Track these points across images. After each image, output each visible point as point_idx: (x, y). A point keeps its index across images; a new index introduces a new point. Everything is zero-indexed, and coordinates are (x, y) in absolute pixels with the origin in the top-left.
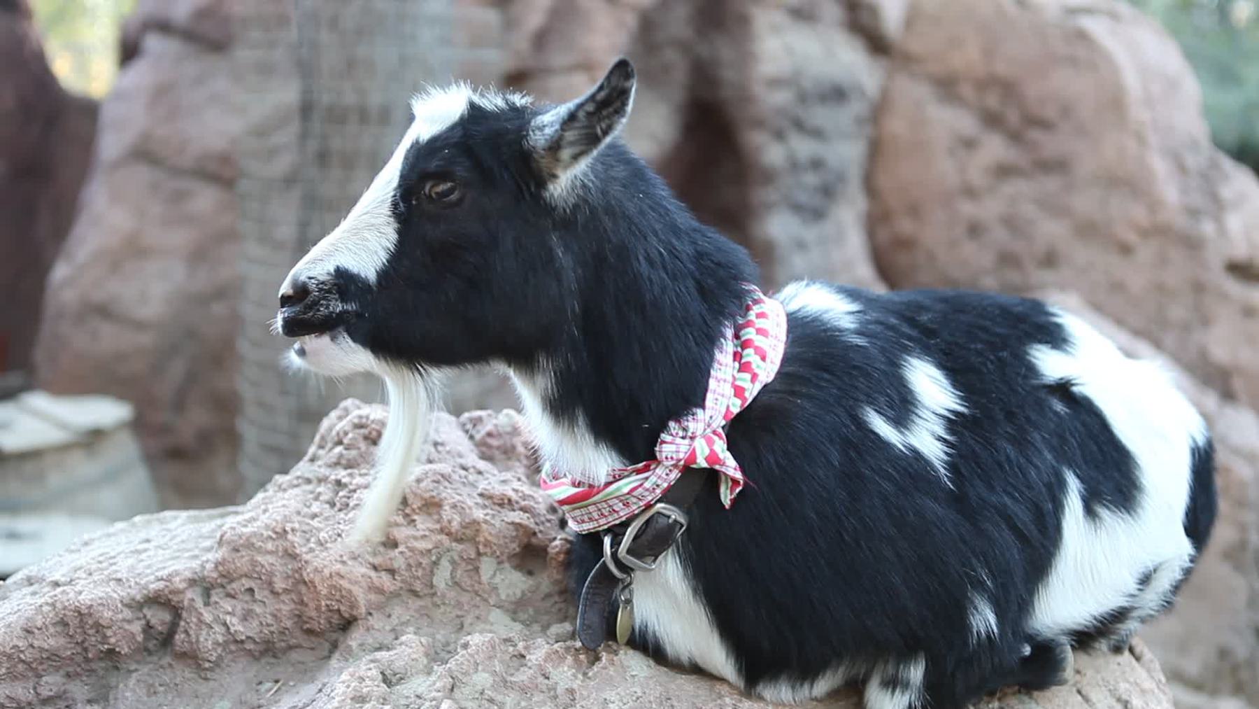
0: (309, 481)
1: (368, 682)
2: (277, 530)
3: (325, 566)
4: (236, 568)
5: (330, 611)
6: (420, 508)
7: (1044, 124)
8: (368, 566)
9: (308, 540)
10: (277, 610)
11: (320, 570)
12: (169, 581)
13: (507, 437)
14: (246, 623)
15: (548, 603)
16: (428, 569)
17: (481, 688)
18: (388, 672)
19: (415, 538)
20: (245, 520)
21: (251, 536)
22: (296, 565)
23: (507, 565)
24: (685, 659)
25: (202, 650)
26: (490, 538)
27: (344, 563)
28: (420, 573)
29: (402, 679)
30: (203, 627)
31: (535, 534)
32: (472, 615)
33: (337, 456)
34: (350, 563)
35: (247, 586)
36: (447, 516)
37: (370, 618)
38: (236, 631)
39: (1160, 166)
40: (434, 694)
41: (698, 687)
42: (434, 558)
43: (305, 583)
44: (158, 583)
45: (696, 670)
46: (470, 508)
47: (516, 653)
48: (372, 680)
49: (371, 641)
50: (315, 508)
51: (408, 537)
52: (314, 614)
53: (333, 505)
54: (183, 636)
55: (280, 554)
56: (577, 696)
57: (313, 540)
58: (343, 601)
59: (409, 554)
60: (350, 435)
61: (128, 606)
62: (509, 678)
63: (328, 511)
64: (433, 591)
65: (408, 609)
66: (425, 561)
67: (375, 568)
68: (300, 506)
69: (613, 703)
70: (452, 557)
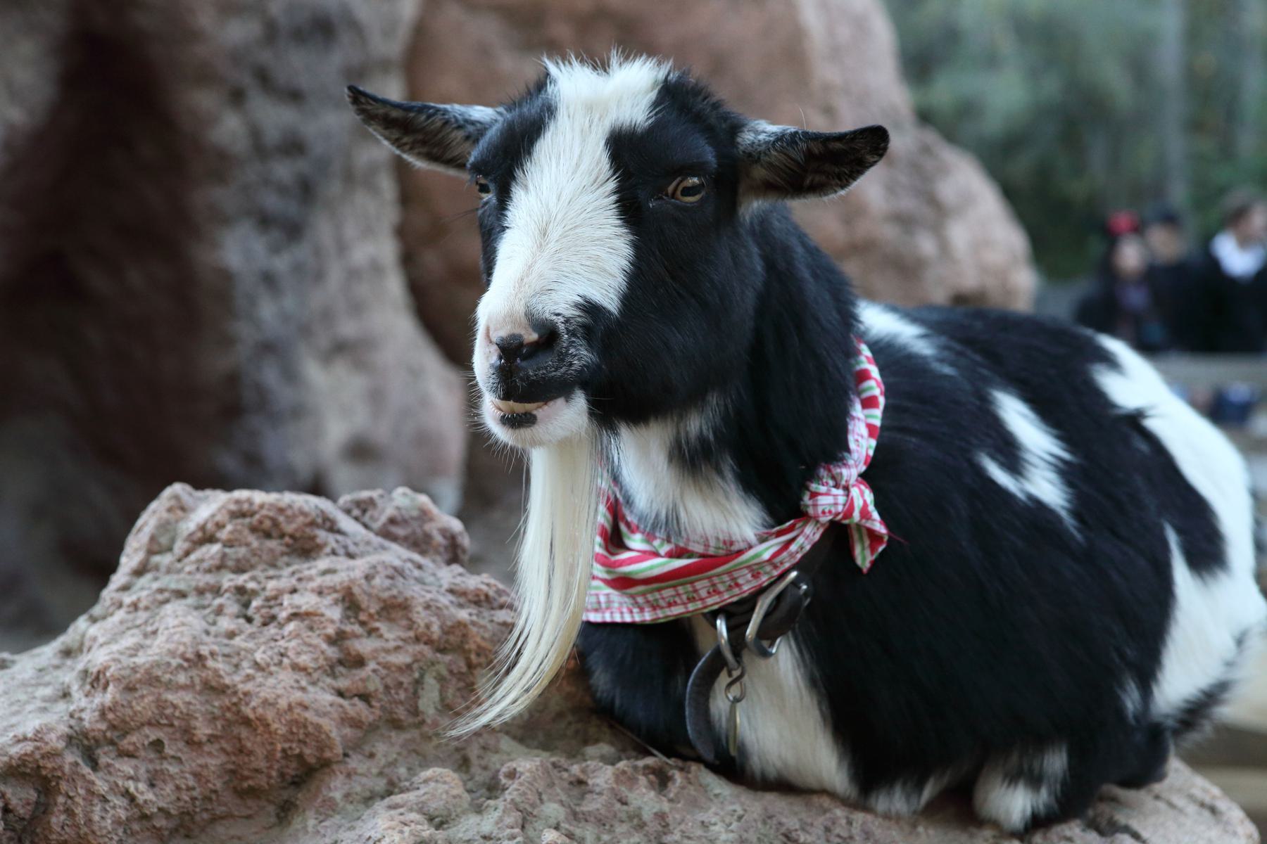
2: (189, 655)
3: (279, 696)
4: (135, 713)
6: (378, 613)
8: (333, 691)
9: (237, 666)
10: (201, 766)
11: (271, 701)
12: (41, 739)
13: (415, 524)
14: (156, 790)
15: (562, 725)
16: (411, 690)
17: (555, 822)
19: (387, 651)
20: (128, 648)
21: (152, 667)
24: (772, 773)
25: (98, 833)
26: (484, 644)
27: (303, 689)
28: (402, 695)
30: (96, 801)
33: (219, 556)
34: (311, 689)
35: (153, 737)
36: (422, 619)
38: (145, 802)
40: (508, 831)
41: (791, 804)
42: (417, 675)
44: (21, 745)
45: (784, 786)
46: (447, 607)
47: (572, 779)
49: (358, 789)
50: (225, 623)
51: (376, 651)
52: (262, 764)
53: (249, 620)
54: (63, 817)
55: (198, 688)
56: (670, 820)
57: (245, 664)
58: (308, 740)
59: (384, 672)
60: (229, 527)
62: (578, 809)
64: (420, 718)
65: (392, 744)
66: (406, 680)
67: (340, 694)
68: (204, 625)
69: (715, 824)
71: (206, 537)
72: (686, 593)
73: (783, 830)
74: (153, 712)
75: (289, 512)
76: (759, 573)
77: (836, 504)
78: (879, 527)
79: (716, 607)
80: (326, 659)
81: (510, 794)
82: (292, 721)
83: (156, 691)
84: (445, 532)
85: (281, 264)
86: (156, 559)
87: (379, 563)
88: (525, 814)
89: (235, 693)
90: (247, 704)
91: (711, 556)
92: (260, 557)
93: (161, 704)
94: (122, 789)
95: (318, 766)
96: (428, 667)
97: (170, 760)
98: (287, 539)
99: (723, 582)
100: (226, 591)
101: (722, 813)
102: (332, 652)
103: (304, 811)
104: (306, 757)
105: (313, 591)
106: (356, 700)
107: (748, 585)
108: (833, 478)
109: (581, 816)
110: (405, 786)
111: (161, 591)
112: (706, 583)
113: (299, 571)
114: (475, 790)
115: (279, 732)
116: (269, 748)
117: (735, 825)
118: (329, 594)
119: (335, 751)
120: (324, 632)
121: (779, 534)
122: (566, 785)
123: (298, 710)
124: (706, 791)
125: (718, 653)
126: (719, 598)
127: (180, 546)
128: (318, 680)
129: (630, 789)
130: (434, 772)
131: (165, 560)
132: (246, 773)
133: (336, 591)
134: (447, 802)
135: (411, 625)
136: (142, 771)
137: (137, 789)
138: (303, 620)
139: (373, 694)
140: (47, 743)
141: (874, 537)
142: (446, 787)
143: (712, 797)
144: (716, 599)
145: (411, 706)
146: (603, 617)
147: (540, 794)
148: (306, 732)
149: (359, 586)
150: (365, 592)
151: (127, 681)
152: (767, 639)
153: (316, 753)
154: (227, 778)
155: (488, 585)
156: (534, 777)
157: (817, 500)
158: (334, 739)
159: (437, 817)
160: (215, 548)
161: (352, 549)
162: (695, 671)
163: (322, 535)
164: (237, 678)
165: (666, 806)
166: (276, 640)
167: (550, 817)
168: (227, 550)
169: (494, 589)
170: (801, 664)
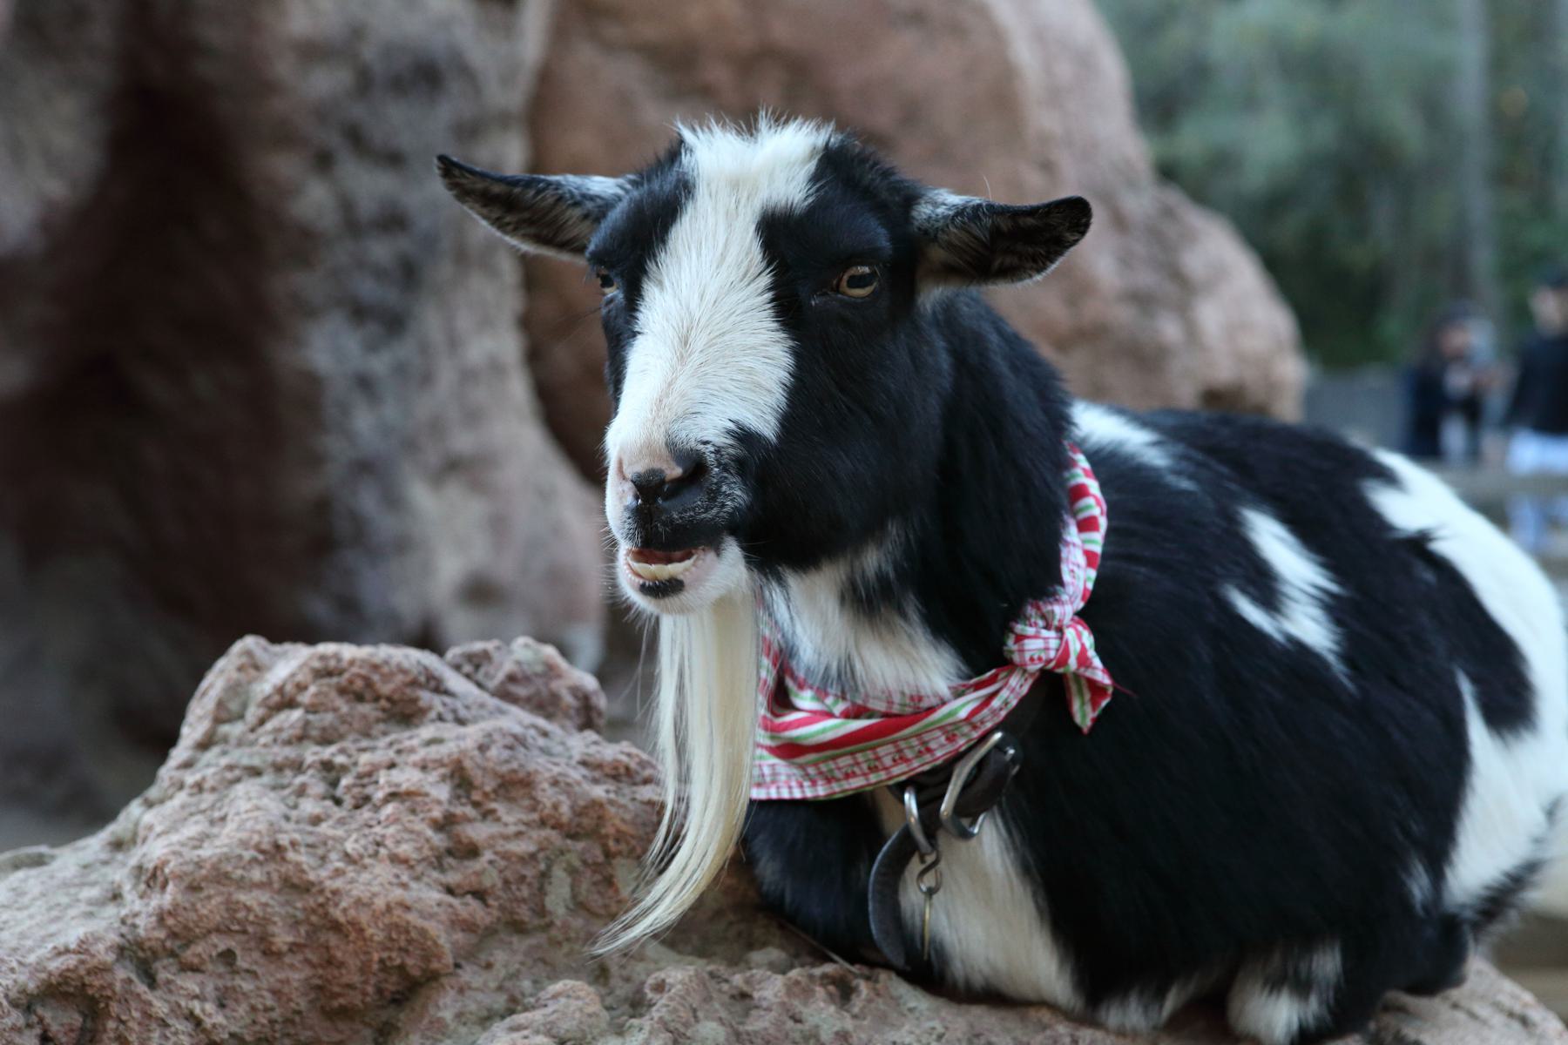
2: (266, 846)
3: (375, 895)
4: (201, 917)
6: (495, 791)
8: (440, 888)
9: (323, 859)
10: (282, 982)
11: (365, 900)
12: (87, 951)
13: (539, 682)
14: (228, 1012)
16: (536, 885)
19: (506, 838)
20: (191, 839)
21: (220, 861)
22: (311, 902)
24: (978, 981)
26: (624, 827)
27: (404, 886)
28: (525, 892)
30: (154, 1026)
33: (300, 724)
34: (413, 885)
35: (222, 947)
37: (459, 971)
38: (214, 1026)
41: (1003, 1019)
42: (542, 866)
44: (62, 959)
46: (579, 784)
47: (735, 992)
49: (473, 1007)
50: (309, 807)
51: (492, 837)
52: (356, 979)
53: (338, 802)
55: (276, 886)
57: (333, 856)
58: (411, 948)
59: (503, 863)
60: (313, 689)
61: (15, 1004)
62: (741, 1028)
64: (547, 920)
65: (514, 952)
67: (450, 890)
68: (283, 809)
70: (569, 863)
71: (284, 701)
72: (866, 761)
74: (222, 917)
75: (386, 669)
76: (954, 735)
77: (1047, 649)
78: (1102, 677)
79: (903, 778)
80: (432, 849)
81: (658, 1011)
82: (391, 924)
83: (224, 889)
84: (576, 691)
85: (379, 364)
86: (225, 729)
87: (495, 730)
88: (676, 1036)
89: (322, 892)
90: (336, 905)
91: (896, 716)
92: (351, 724)
93: (233, 906)
94: (186, 1011)
95: (423, 980)
96: (557, 856)
97: (243, 974)
98: (383, 703)
99: (911, 747)
100: (309, 767)
101: (918, 1031)
103: (407, 1035)
104: (408, 969)
105: (415, 765)
106: (469, 898)
107: (941, 752)
108: (1043, 617)
109: (745, 1037)
110: (529, 1003)
111: (230, 768)
112: (890, 748)
113: (398, 741)
114: (615, 1006)
115: (376, 938)
116: (363, 957)
118: (434, 769)
119: (443, 961)
120: (429, 815)
121: (978, 687)
122: (726, 998)
123: (398, 912)
124: (898, 1005)
125: (907, 834)
126: (908, 766)
127: (253, 713)
128: (423, 874)
129: (805, 1004)
130: (565, 985)
131: (235, 730)
132: (336, 989)
133: (443, 765)
134: (581, 1022)
135: (535, 806)
136: (210, 988)
137: (203, 1011)
138: (403, 802)
139: (490, 891)
140: (93, 956)
141: (1096, 689)
142: (580, 1003)
143: (906, 1012)
144: (903, 768)
145: (537, 905)
146: (768, 793)
147: (694, 1011)
148: (409, 938)
149: (472, 758)
150: (479, 767)
151: (191, 878)
152: (967, 816)
153: (419, 963)
154: (312, 995)
155: (629, 755)
156: (687, 989)
157: (1023, 645)
158: (443, 947)
159: (569, 1040)
160: (296, 715)
161: (463, 713)
162: (880, 857)
163: (425, 697)
164: (324, 873)
165: (849, 1024)
166: (371, 827)
167: (707, 1039)
168: (311, 717)
169: (637, 760)
170: (1010, 847)
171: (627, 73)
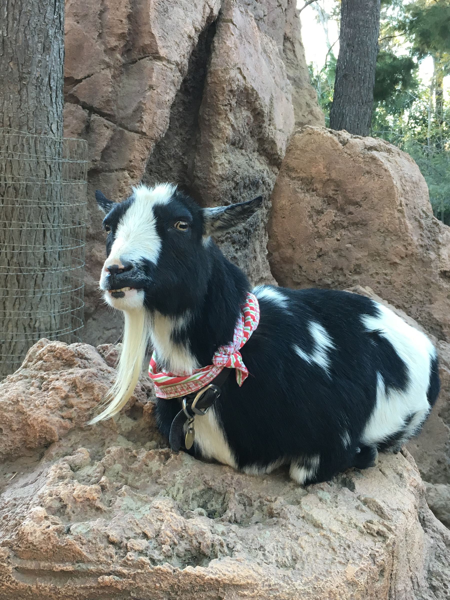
0: (26, 377)
1: (64, 470)
5: (41, 438)
6: (83, 389)
7: (357, 204)
9: (30, 405)
15: (144, 433)
18: (73, 465)
19: (82, 403)
22: (24, 417)
23: (125, 415)
27: (48, 415)
29: (79, 468)
31: (137, 401)
32: (109, 438)
34: (51, 415)
39: (410, 225)
43: (29, 425)
45: (214, 461)
48: (66, 468)
49: (62, 452)
50: (32, 389)
51: (78, 403)
52: (32, 440)
53: (40, 388)
56: (161, 473)
57: (32, 405)
63: (38, 391)
67: (63, 417)
68: (24, 389)
73: (204, 480)
75: (66, 351)
102: (62, 402)
117: (186, 476)
129: (151, 461)
133: (70, 381)
150: (79, 382)
171: (296, 185)
